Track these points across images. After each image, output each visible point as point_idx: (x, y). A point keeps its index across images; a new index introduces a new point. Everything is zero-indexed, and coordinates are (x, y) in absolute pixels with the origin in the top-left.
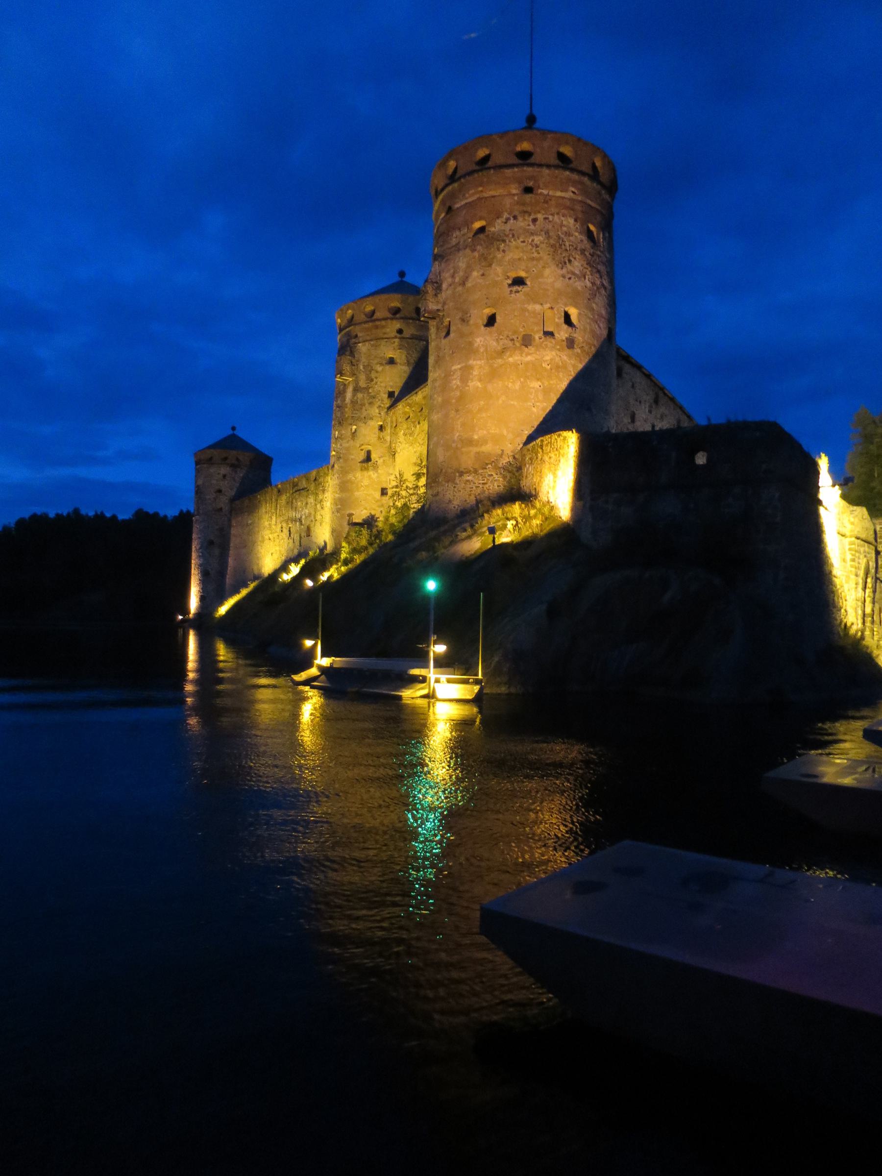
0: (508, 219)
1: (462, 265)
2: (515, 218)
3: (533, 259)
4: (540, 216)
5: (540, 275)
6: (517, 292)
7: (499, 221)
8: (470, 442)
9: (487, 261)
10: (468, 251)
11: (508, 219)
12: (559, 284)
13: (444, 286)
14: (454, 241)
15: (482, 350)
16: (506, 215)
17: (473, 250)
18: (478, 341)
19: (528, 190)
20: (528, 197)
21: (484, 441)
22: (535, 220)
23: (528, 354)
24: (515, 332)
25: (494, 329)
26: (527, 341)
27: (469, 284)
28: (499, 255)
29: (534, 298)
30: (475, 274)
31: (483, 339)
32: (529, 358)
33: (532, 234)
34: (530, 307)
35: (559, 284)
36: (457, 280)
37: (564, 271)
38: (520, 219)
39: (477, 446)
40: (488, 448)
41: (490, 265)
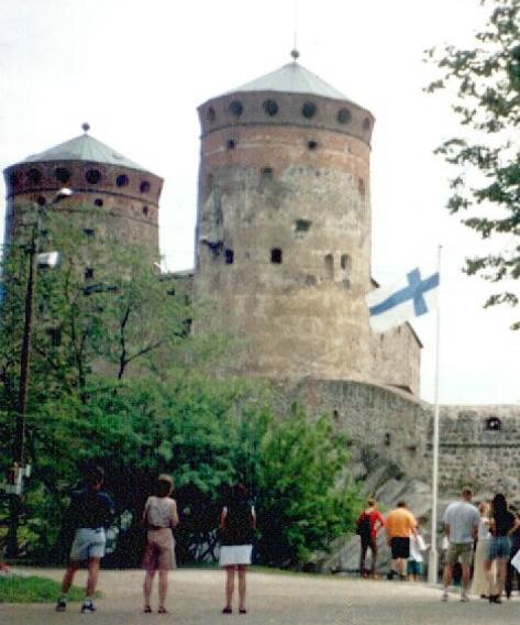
0: (293, 171)
1: (248, 204)
2: (301, 170)
3: (314, 209)
4: (322, 170)
5: (319, 226)
6: (302, 237)
7: (286, 172)
8: (255, 368)
9: (274, 205)
10: (255, 192)
11: (293, 171)
12: (338, 232)
13: (226, 217)
14: (237, 178)
15: (268, 285)
16: (291, 166)
17: (262, 192)
18: (264, 278)
19: (312, 145)
20: (313, 155)
21: (269, 367)
22: (318, 174)
23: (311, 293)
24: (301, 274)
25: (281, 266)
26: (311, 280)
27: (257, 223)
28: (287, 201)
29: (319, 243)
30: (262, 215)
31: (269, 274)
32: (311, 298)
33: (315, 187)
34: (313, 252)
35: (338, 232)
36: (243, 216)
37: (342, 222)
38: (305, 172)
39: (261, 372)
40: (274, 374)
41: (277, 208)
